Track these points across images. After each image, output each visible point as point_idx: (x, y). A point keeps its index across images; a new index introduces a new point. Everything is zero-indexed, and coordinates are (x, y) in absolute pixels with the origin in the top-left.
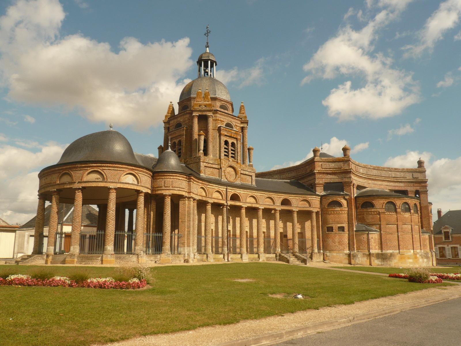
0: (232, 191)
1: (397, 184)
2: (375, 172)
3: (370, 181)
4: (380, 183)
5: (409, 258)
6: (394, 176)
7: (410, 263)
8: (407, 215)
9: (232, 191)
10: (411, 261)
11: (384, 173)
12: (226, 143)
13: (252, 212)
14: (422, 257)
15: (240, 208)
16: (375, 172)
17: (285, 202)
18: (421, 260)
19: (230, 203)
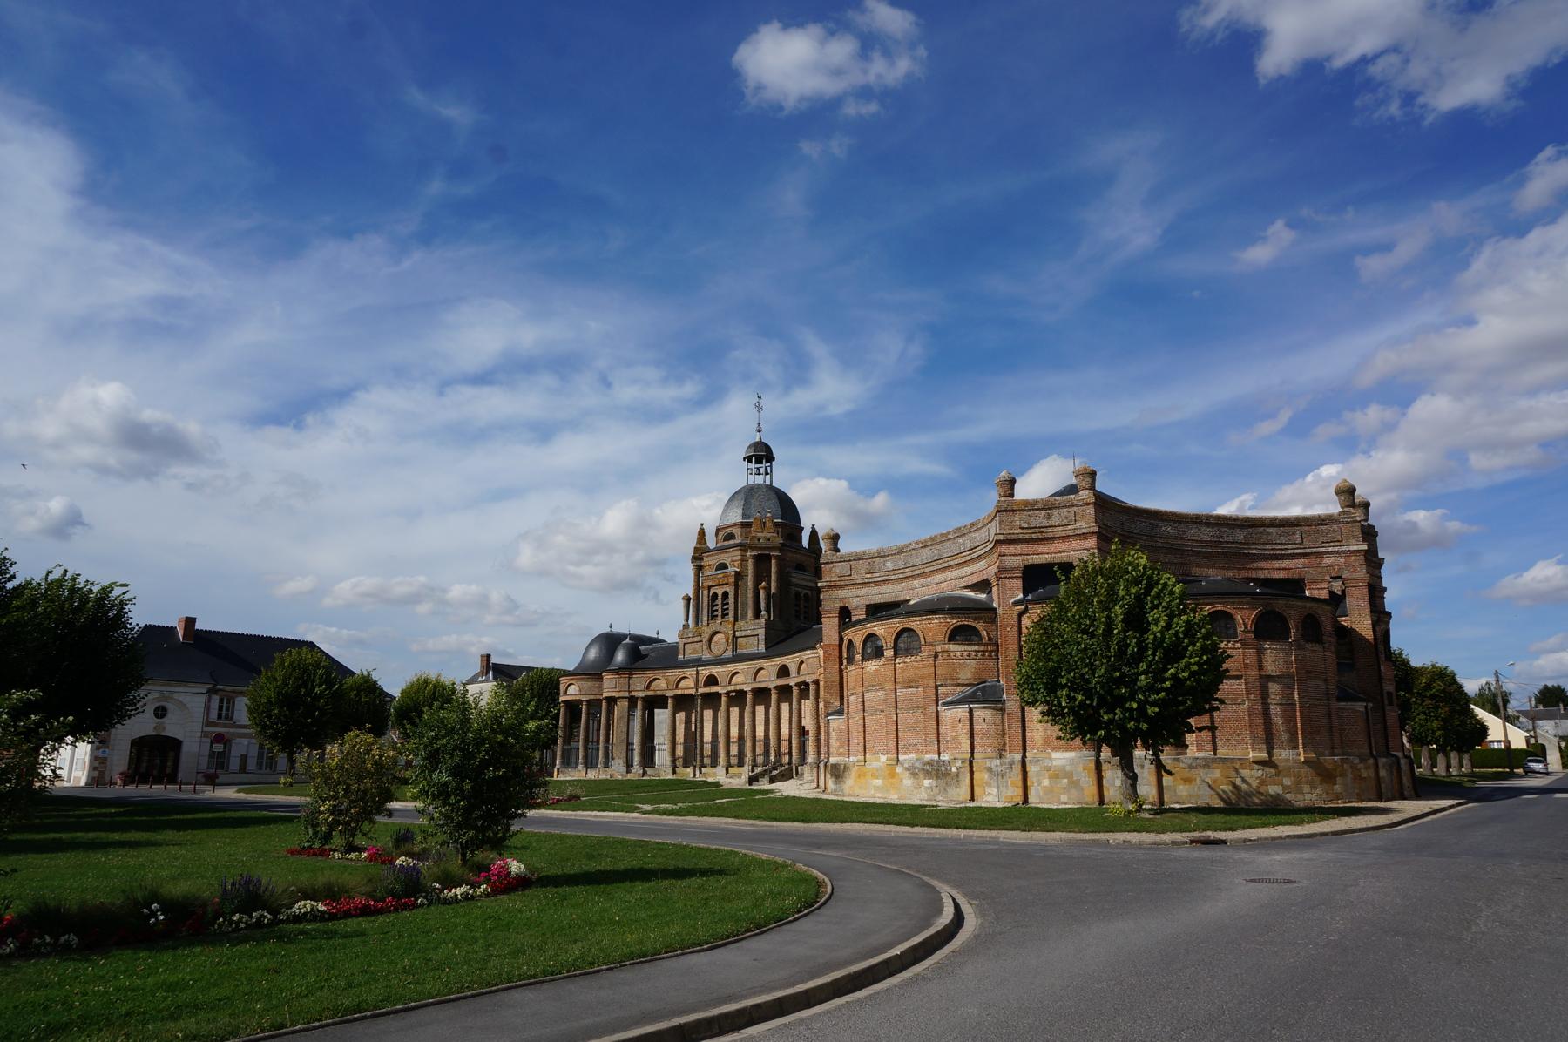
0: (705, 672)
1: (967, 570)
2: (926, 554)
3: (915, 583)
4: (939, 577)
5: (874, 776)
6: (968, 546)
7: (877, 788)
8: (872, 666)
9: (705, 672)
10: (878, 782)
11: (947, 549)
12: (715, 595)
13: (738, 698)
14: (914, 775)
15: (718, 695)
16: (926, 554)
17: (784, 671)
18: (908, 782)
19: (702, 690)
